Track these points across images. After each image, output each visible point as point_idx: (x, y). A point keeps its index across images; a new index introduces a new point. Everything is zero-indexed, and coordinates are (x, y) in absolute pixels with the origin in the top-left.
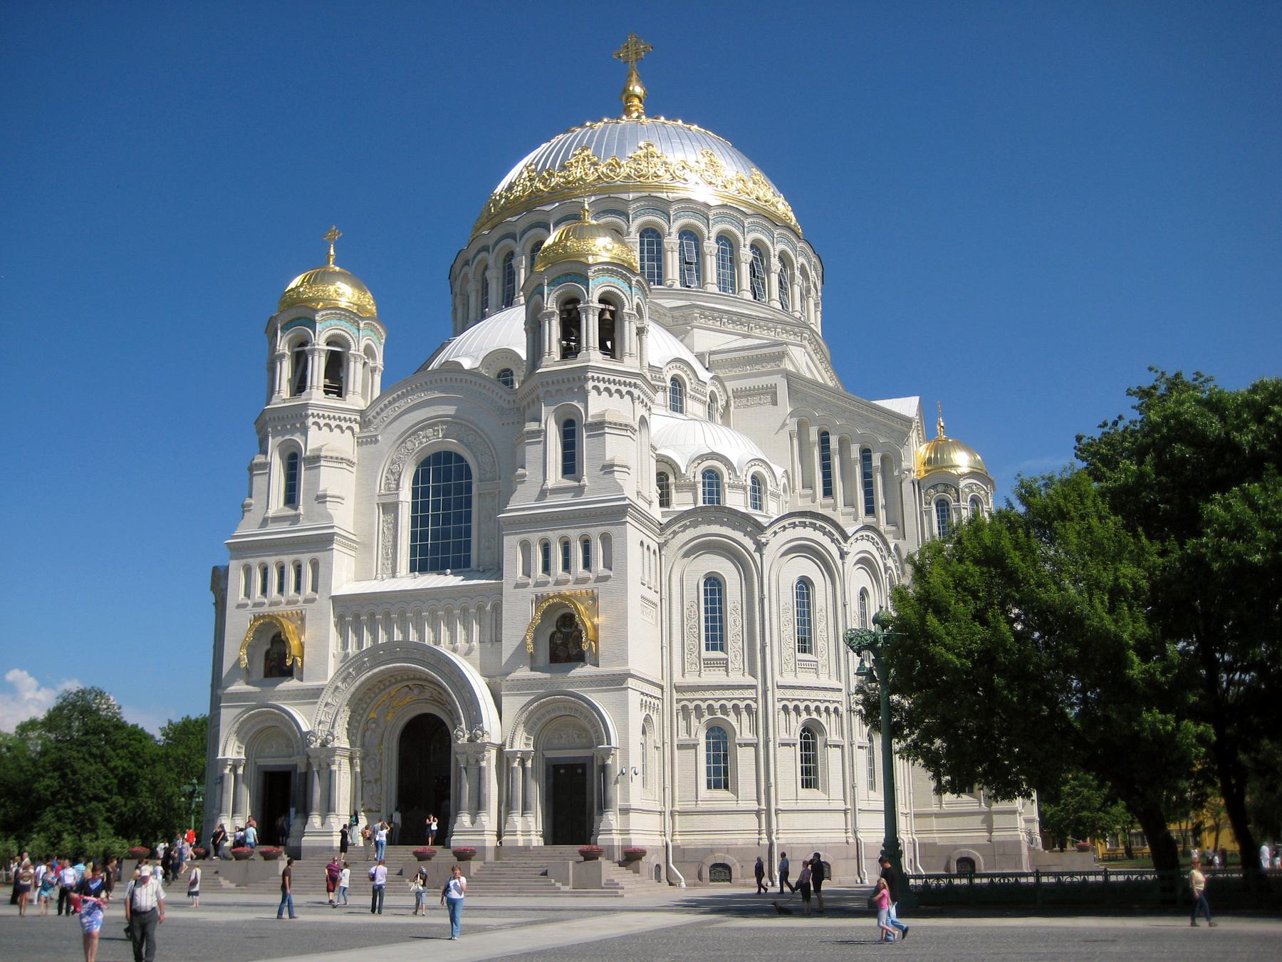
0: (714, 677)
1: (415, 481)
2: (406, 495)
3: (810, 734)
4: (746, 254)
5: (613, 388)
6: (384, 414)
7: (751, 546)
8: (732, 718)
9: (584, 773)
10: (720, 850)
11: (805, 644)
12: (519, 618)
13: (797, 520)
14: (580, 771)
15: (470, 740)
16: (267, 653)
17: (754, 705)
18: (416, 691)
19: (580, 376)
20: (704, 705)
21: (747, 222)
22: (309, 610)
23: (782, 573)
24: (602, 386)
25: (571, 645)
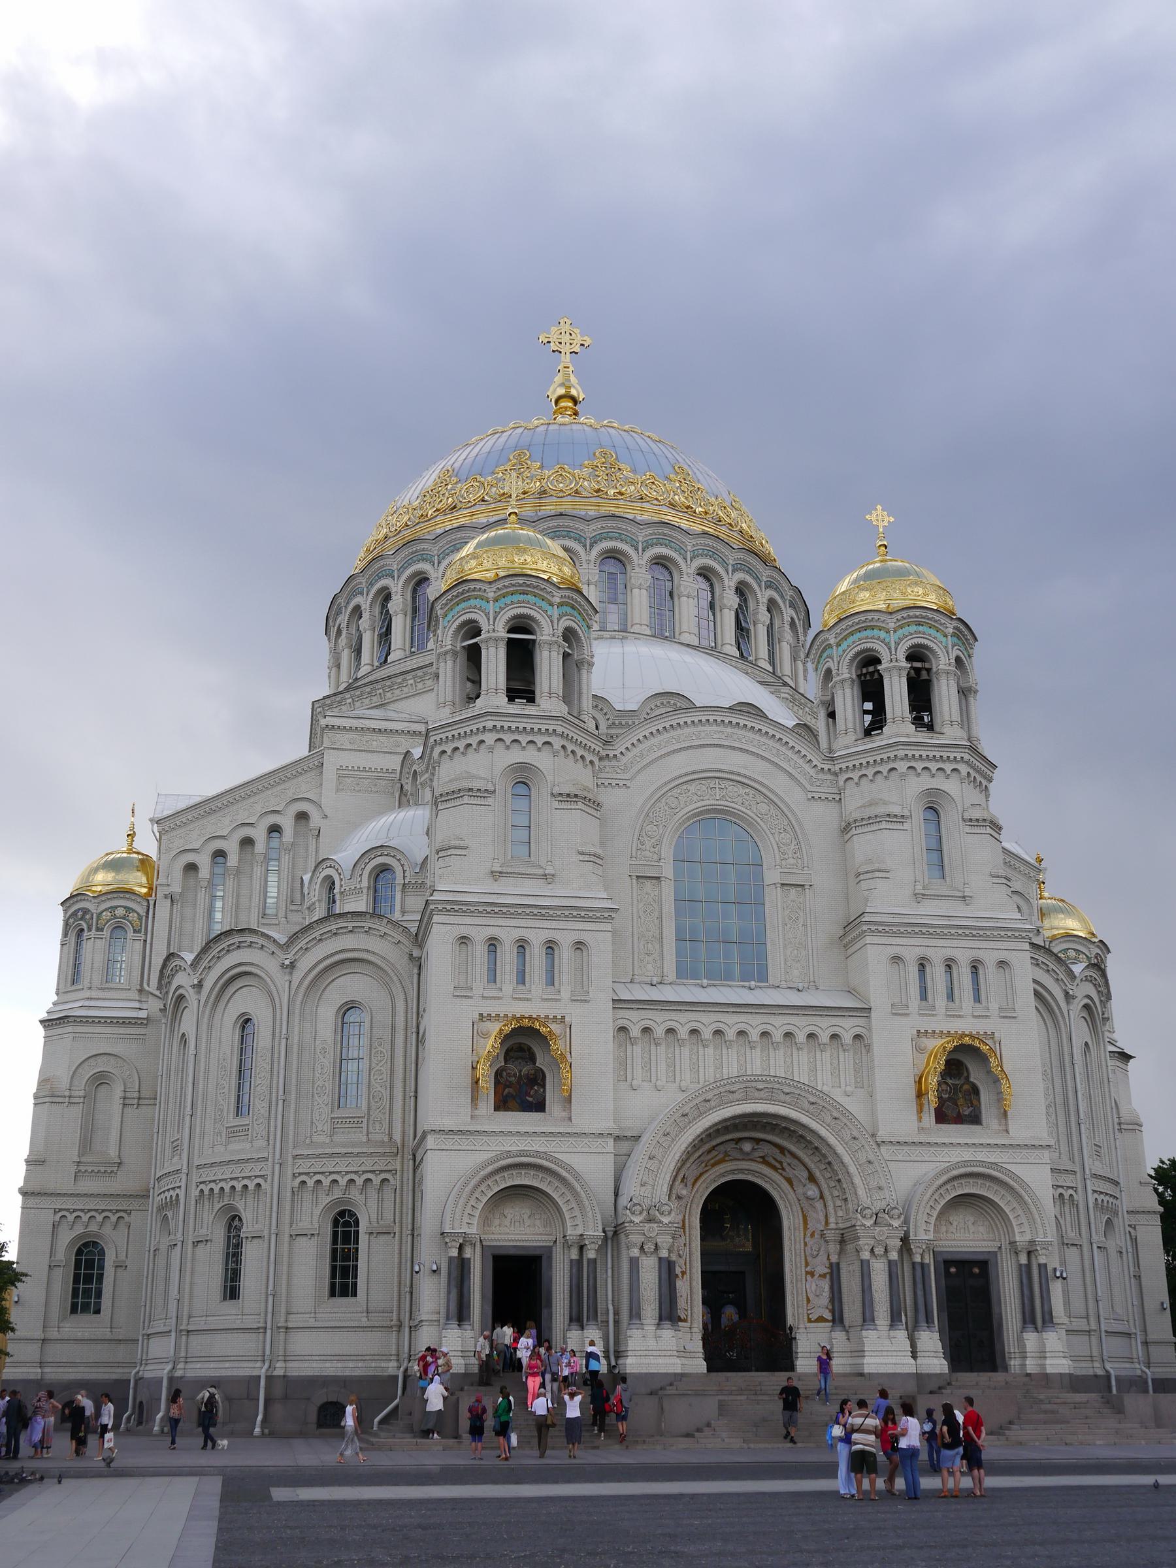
2: (668, 871)
6: (635, 751)
7: (1060, 996)
12: (901, 1055)
14: (976, 1270)
18: (747, 1147)
22: (574, 1014)
24: (973, 774)
25: (961, 1102)
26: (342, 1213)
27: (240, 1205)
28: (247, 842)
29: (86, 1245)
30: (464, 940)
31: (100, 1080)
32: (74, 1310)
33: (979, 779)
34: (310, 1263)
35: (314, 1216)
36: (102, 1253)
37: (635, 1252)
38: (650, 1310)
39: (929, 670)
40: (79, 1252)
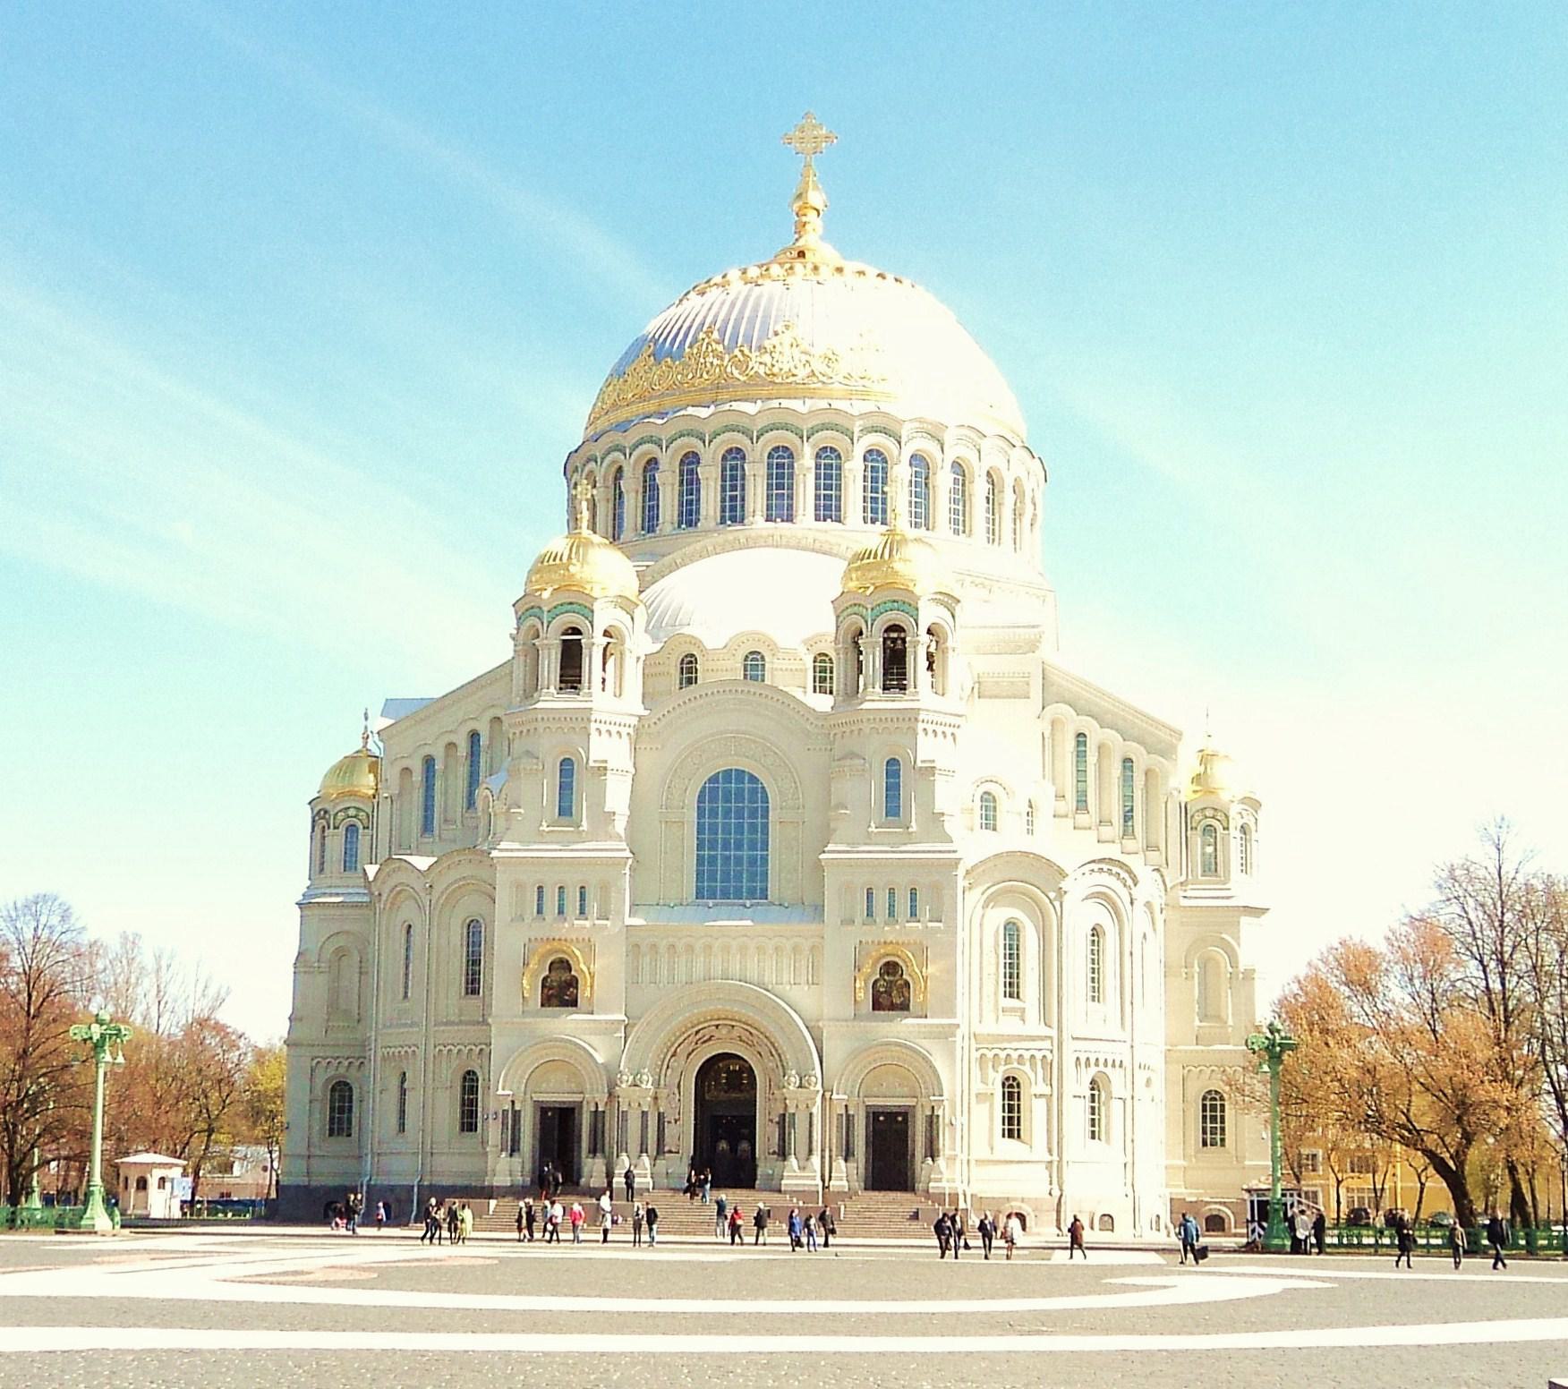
0: (1010, 1025)
1: (701, 800)
3: (1094, 1084)
4: (979, 488)
5: (939, 729)
8: (1027, 1068)
9: (905, 1121)
10: (1015, 1199)
11: (1096, 994)
13: (1096, 867)
15: (800, 1086)
16: (545, 979)
17: (1049, 1057)
19: (911, 717)
20: (1003, 1055)
21: (985, 445)
23: (1079, 915)
24: (930, 728)
26: (468, 1073)
27: (404, 1065)
28: (451, 746)
29: (339, 1083)
30: (519, 886)
31: (341, 953)
32: (331, 1135)
33: (939, 729)
34: (447, 1109)
35: (450, 1077)
36: (351, 1089)
37: (624, 1108)
38: (634, 1145)
39: (904, 641)
40: (333, 1089)
